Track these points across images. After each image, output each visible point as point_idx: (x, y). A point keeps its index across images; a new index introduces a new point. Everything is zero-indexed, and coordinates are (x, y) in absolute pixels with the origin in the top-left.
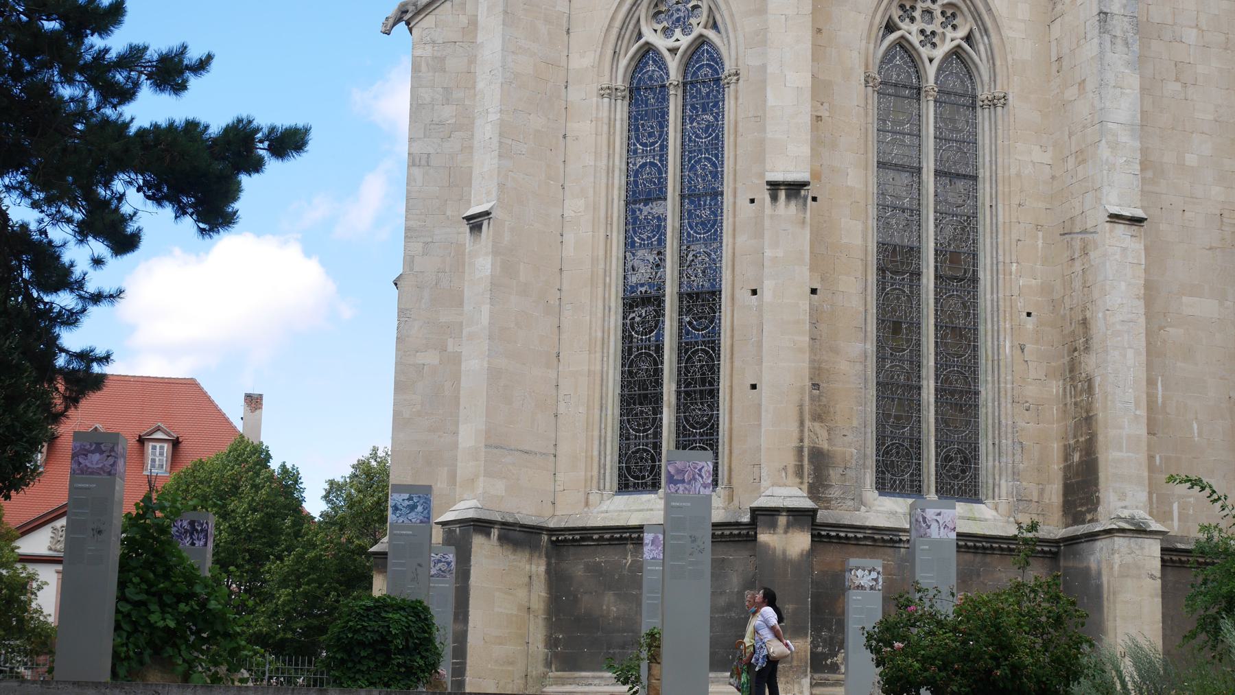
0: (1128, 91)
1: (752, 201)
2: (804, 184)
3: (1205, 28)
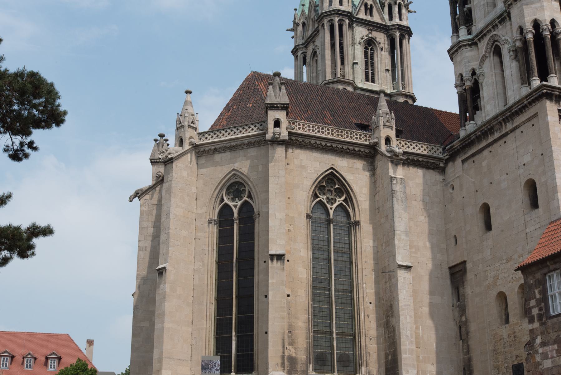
0: (403, 219)
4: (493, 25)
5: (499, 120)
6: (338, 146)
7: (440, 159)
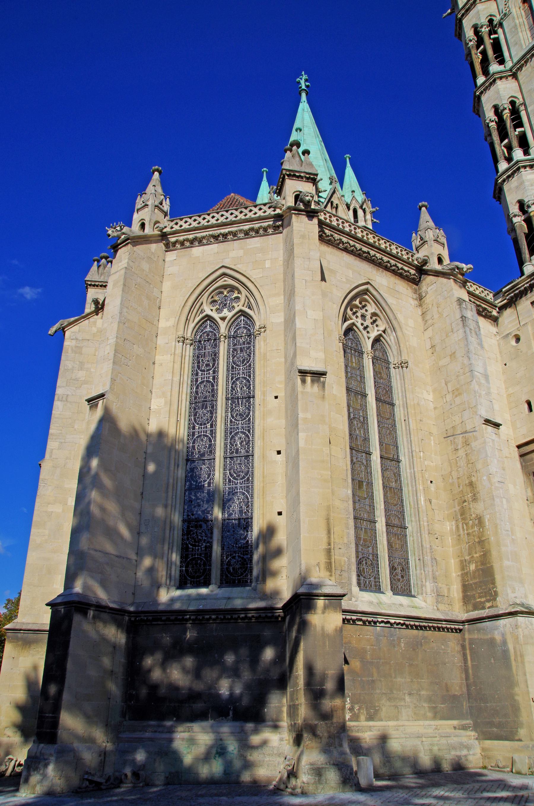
0: (481, 357)
1: (276, 397)
2: (324, 374)
3: (487, 350)
6: (376, 256)
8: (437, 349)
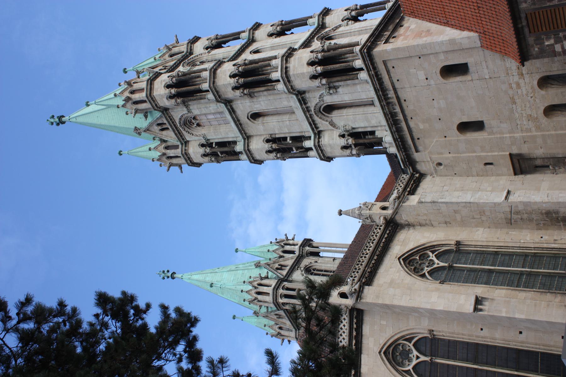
1: (482, 329)
2: (477, 298)
4: (306, 110)
5: (385, 104)
7: (412, 175)
8: (448, 220)
